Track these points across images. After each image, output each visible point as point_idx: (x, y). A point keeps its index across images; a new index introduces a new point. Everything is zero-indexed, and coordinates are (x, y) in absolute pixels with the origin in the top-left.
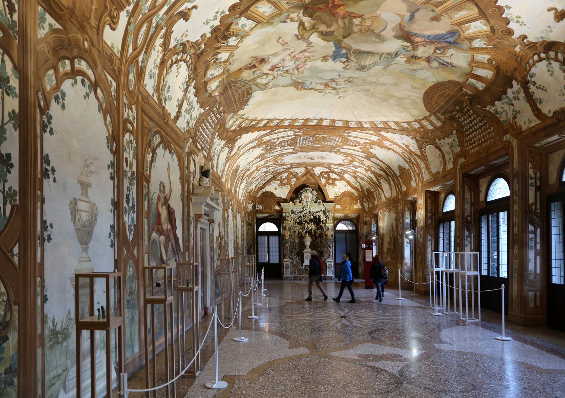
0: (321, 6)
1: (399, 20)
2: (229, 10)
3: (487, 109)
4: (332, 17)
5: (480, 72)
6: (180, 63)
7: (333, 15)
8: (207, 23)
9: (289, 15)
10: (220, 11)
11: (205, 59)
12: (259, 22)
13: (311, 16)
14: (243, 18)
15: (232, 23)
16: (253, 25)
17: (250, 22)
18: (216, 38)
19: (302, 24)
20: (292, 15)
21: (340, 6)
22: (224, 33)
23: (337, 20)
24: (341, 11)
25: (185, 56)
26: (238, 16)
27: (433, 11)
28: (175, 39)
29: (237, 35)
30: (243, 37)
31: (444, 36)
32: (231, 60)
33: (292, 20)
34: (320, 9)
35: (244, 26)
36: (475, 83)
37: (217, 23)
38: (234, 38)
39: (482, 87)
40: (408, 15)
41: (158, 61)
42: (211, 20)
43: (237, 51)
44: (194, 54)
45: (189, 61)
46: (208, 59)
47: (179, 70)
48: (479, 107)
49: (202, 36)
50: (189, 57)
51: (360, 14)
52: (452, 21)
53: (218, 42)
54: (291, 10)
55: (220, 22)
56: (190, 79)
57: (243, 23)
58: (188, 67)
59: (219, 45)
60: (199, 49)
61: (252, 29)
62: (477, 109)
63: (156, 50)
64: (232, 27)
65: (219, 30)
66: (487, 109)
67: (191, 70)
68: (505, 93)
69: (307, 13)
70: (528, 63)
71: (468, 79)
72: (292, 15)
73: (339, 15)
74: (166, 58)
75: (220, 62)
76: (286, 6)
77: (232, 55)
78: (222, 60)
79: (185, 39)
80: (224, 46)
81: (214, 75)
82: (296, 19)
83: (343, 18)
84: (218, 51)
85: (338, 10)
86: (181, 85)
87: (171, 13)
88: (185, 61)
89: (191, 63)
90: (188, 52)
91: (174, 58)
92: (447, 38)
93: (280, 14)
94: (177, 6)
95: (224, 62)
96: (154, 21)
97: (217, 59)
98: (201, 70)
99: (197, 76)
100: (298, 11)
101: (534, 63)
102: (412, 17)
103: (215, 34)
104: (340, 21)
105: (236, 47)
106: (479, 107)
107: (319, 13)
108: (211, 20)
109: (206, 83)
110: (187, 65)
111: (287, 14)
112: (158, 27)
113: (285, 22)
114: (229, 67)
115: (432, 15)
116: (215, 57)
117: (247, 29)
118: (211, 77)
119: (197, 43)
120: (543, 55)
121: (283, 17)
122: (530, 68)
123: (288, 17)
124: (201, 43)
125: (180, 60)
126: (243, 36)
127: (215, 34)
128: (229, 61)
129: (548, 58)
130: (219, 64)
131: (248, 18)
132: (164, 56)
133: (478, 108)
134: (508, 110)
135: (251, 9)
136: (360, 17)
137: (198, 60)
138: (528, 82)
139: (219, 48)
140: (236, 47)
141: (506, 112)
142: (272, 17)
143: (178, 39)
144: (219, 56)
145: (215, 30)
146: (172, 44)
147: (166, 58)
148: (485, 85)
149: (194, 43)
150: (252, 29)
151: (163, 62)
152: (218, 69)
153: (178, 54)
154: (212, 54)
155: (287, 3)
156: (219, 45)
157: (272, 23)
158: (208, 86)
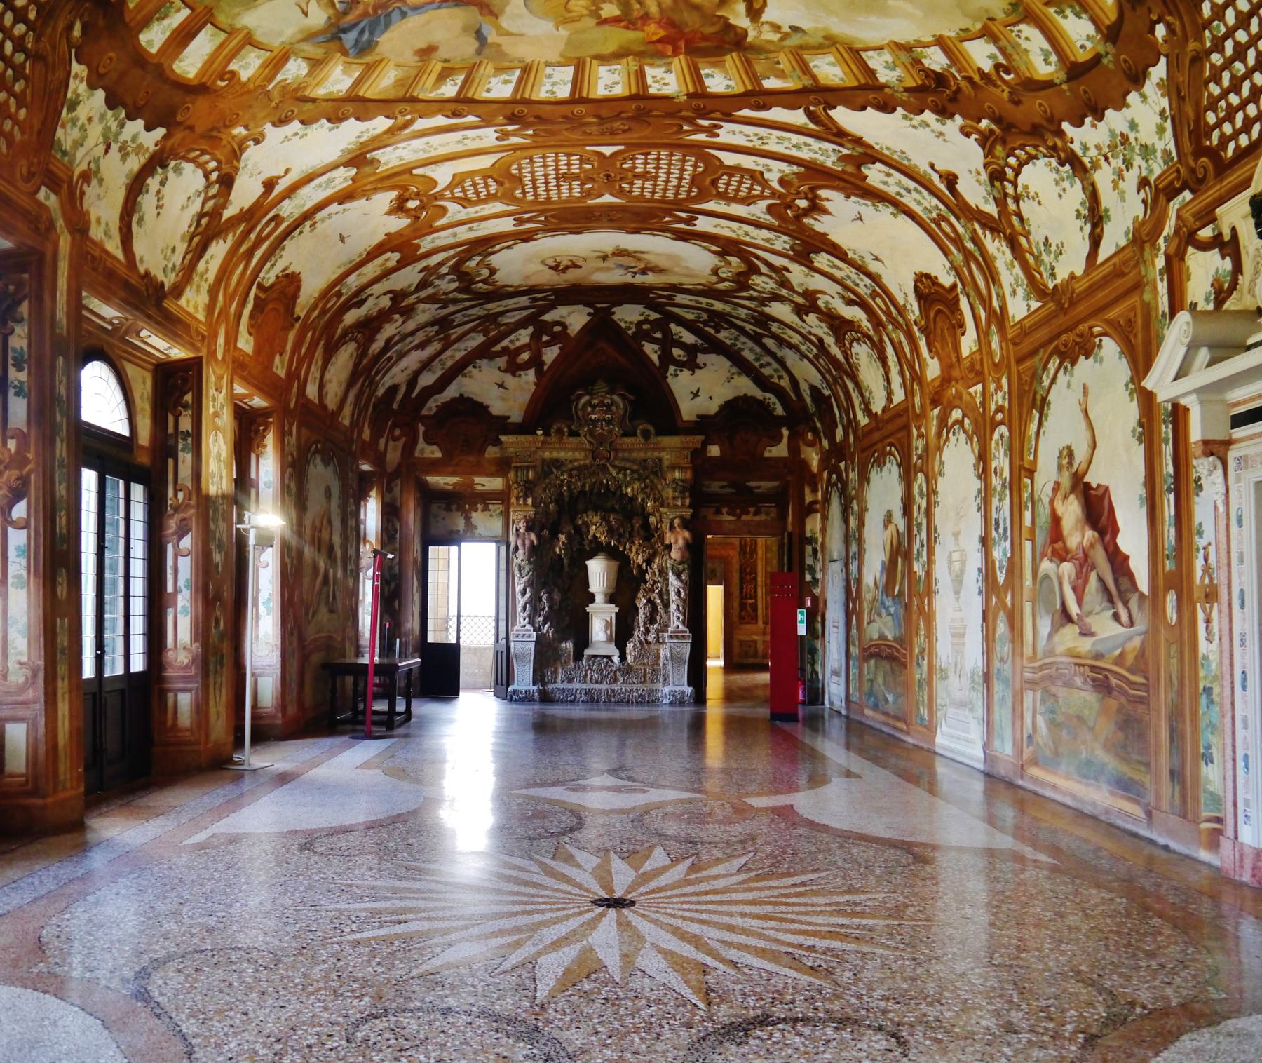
0: (703, 44)
1: (504, 22)
2: (893, 110)
3: (76, 68)
4: (676, 17)
5: (202, 47)
6: (1020, 189)
7: (671, 24)
8: (941, 134)
9: (782, 39)
10: (907, 123)
11: (1010, 106)
12: (854, 54)
13: (728, 27)
14: (882, 80)
15: (907, 90)
16: (870, 53)
17: (871, 64)
19: (754, 13)
20: (775, 37)
21: (659, 41)
22: (934, 91)
23: (661, 10)
24: (654, 31)
25: (1009, 171)
26: (887, 90)
27: (446, 61)
28: (986, 201)
29: (917, 62)
30: (907, 48)
31: (372, 33)
32: (978, 26)
33: (777, 28)
34: (705, 38)
35: (891, 67)
36: (166, 22)
37: (928, 116)
38: (926, 62)
39: (150, 42)
40: (492, 37)
41: (1009, 255)
42: (933, 131)
43: (946, 33)
44: (1004, 143)
45: (1018, 158)
46: (1005, 95)
47: (1032, 194)
48: (77, 31)
49: (968, 135)
50: (1012, 160)
51: (607, 27)
52: (391, 64)
53: (959, 90)
54: (772, 48)
55: (922, 112)
57: (887, 72)
58: (1031, 158)
59: (964, 84)
60: (992, 131)
61: (879, 49)
62: (61, 25)
63: (996, 254)
64: (910, 83)
65: (937, 105)
66: (76, 68)
67: (1036, 147)
68: (131, 117)
69: (736, 34)
70: (203, 152)
71: (188, 6)
72: (775, 37)
73: (659, 23)
74: (1008, 231)
76: (782, 57)
78: (992, 49)
79: (984, 177)
80: (959, 71)
82: (766, 27)
83: (646, 17)
84: (977, 78)
85: (662, 33)
86: (1058, 189)
88: (1017, 173)
89: (1022, 147)
90: (1002, 162)
91: (1012, 206)
92: (362, 32)
93: (801, 47)
95: (994, 39)
96: (970, 245)
97: (998, 66)
98: (1036, 106)
99: (1051, 120)
100: (757, 42)
101: (201, 166)
102: (479, 35)
103: (950, 107)
104: (654, 9)
105: (940, 41)
106: (77, 31)
107: (709, 30)
108: (933, 131)
109: (1076, 71)
110: (1027, 163)
111: (787, 43)
112: (975, 240)
113: (795, 29)
115: (442, 53)
116: (994, 77)
117: (887, 57)
118: (1053, 58)
119: (986, 141)
120: (214, 176)
121: (795, 40)
122: (193, 161)
123: (785, 37)
124: (979, 132)
125: (1015, 185)
126: (906, 51)
127: (950, 107)
129: (208, 187)
130: (1010, 50)
131: (871, 73)
132: (1006, 237)
133: (70, 27)
134: (90, 143)
135: (855, 84)
136: (604, 22)
138: (164, 166)
139: (969, 79)
140: (940, 41)
141: (84, 137)
142: (819, 49)
143: (985, 194)
144: (987, 66)
145: (944, 113)
146: (991, 209)
147: (1008, 231)
148: (154, 50)
149: (984, 149)
150: (879, 49)
151: (1013, 244)
153: (1006, 195)
154: (992, 89)
155: (778, 63)
156: (964, 84)
157: (825, 38)
158: (1082, 57)
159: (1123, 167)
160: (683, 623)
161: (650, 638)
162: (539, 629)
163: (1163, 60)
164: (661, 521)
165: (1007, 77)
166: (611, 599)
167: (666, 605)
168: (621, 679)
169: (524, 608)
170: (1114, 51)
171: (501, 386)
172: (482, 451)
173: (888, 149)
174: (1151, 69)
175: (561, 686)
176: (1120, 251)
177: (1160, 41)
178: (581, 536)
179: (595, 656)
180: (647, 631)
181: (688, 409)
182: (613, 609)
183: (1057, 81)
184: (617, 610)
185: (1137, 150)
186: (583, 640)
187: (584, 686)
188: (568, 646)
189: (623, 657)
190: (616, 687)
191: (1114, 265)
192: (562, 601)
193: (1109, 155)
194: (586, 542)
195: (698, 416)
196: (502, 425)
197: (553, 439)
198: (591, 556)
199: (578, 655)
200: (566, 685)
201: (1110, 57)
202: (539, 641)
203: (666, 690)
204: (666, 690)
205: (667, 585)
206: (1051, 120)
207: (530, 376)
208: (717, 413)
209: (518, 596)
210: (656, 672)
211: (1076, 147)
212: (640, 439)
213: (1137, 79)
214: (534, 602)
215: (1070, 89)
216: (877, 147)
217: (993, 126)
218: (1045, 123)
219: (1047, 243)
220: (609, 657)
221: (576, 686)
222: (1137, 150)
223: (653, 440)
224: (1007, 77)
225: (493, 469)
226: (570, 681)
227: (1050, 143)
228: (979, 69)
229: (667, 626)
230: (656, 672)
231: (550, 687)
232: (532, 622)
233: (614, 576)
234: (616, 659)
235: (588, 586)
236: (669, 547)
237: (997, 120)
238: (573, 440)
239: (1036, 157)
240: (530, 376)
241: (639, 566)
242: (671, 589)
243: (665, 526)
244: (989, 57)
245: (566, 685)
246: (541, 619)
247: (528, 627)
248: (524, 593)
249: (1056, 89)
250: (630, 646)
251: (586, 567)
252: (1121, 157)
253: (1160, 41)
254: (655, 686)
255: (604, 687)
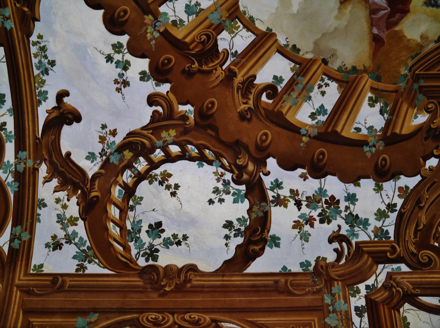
18: (189, 74)
56: (242, 169)
58: (201, 159)
75: (292, 82)
77: (289, 53)
80: (234, 63)
81: (329, 107)
87: (30, 141)
94: (28, 124)
114: (335, 65)
124: (170, 109)
128: (312, 61)
137: (215, 129)
139: (231, 75)
152: (315, 93)
159: (318, 219)
163: (418, 178)
165: (264, 98)
170: (381, 148)
173: (43, 49)
174: (402, 177)
176: (285, 273)
177: (427, 167)
183: (303, 131)
185: (343, 214)
191: (276, 282)
193: (304, 203)
201: (374, 149)
206: (259, 148)
211: (267, 181)
213: (382, 175)
215: (307, 144)
216: (34, 38)
217: (192, 116)
218: (252, 148)
219: (156, 228)
222: (343, 214)
224: (264, 98)
227: (239, 162)
228: (254, 77)
237: (200, 113)
239: (210, 163)
244: (275, 77)
249: (297, 136)
252: (319, 211)
253: (427, 167)
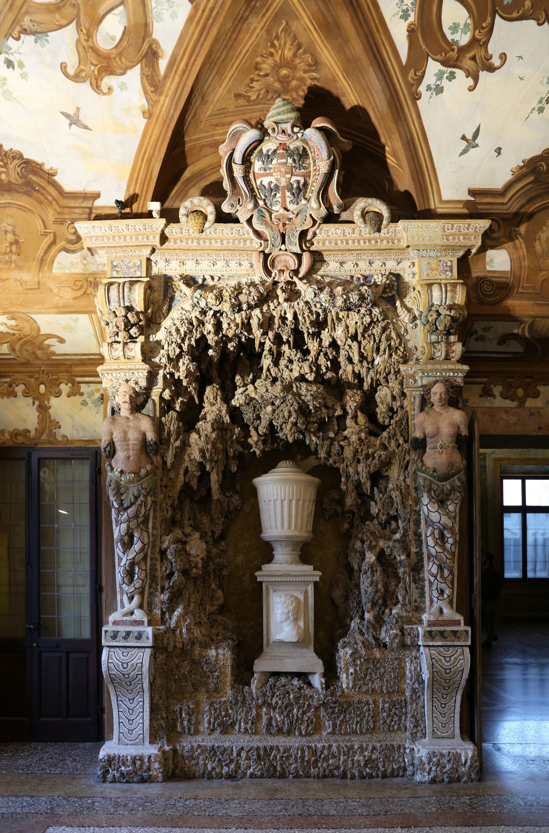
160: (451, 603)
161: (387, 635)
162: (163, 621)
164: (404, 395)
166: (305, 552)
167: (417, 568)
168: (328, 724)
169: (130, 574)
171: (74, 120)
172: (44, 262)
175: (206, 740)
178: (245, 428)
179: (277, 674)
180: (379, 621)
181: (454, 177)
182: (310, 573)
184: (317, 576)
186: (250, 642)
187: (255, 741)
188: (221, 655)
189: (331, 673)
190: (319, 743)
192: (208, 559)
194: (254, 438)
195: (472, 192)
196: (86, 206)
197: (184, 229)
198: (267, 464)
199: (243, 671)
200: (217, 740)
202: (159, 647)
203: (422, 750)
204: (422, 750)
205: (417, 523)
207: (130, 86)
208: (509, 186)
209: (118, 550)
210: (398, 707)
212: (362, 229)
214: (154, 555)
220: (303, 676)
221: (237, 741)
223: (389, 230)
225: (68, 295)
226: (226, 728)
229: (419, 609)
230: (398, 711)
231: (186, 744)
232: (146, 606)
233: (309, 508)
234: (317, 681)
235: (261, 531)
236: (420, 445)
238: (226, 228)
240: (130, 86)
241: (358, 486)
242: (425, 531)
243: (411, 403)
245: (217, 740)
246: (164, 597)
247: (139, 614)
248: (128, 544)
250: (344, 654)
251: (254, 492)
254: (396, 739)
255: (295, 742)
